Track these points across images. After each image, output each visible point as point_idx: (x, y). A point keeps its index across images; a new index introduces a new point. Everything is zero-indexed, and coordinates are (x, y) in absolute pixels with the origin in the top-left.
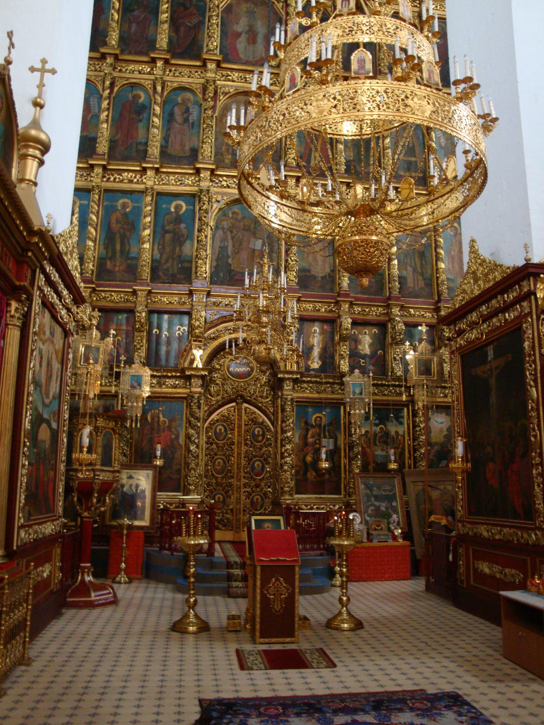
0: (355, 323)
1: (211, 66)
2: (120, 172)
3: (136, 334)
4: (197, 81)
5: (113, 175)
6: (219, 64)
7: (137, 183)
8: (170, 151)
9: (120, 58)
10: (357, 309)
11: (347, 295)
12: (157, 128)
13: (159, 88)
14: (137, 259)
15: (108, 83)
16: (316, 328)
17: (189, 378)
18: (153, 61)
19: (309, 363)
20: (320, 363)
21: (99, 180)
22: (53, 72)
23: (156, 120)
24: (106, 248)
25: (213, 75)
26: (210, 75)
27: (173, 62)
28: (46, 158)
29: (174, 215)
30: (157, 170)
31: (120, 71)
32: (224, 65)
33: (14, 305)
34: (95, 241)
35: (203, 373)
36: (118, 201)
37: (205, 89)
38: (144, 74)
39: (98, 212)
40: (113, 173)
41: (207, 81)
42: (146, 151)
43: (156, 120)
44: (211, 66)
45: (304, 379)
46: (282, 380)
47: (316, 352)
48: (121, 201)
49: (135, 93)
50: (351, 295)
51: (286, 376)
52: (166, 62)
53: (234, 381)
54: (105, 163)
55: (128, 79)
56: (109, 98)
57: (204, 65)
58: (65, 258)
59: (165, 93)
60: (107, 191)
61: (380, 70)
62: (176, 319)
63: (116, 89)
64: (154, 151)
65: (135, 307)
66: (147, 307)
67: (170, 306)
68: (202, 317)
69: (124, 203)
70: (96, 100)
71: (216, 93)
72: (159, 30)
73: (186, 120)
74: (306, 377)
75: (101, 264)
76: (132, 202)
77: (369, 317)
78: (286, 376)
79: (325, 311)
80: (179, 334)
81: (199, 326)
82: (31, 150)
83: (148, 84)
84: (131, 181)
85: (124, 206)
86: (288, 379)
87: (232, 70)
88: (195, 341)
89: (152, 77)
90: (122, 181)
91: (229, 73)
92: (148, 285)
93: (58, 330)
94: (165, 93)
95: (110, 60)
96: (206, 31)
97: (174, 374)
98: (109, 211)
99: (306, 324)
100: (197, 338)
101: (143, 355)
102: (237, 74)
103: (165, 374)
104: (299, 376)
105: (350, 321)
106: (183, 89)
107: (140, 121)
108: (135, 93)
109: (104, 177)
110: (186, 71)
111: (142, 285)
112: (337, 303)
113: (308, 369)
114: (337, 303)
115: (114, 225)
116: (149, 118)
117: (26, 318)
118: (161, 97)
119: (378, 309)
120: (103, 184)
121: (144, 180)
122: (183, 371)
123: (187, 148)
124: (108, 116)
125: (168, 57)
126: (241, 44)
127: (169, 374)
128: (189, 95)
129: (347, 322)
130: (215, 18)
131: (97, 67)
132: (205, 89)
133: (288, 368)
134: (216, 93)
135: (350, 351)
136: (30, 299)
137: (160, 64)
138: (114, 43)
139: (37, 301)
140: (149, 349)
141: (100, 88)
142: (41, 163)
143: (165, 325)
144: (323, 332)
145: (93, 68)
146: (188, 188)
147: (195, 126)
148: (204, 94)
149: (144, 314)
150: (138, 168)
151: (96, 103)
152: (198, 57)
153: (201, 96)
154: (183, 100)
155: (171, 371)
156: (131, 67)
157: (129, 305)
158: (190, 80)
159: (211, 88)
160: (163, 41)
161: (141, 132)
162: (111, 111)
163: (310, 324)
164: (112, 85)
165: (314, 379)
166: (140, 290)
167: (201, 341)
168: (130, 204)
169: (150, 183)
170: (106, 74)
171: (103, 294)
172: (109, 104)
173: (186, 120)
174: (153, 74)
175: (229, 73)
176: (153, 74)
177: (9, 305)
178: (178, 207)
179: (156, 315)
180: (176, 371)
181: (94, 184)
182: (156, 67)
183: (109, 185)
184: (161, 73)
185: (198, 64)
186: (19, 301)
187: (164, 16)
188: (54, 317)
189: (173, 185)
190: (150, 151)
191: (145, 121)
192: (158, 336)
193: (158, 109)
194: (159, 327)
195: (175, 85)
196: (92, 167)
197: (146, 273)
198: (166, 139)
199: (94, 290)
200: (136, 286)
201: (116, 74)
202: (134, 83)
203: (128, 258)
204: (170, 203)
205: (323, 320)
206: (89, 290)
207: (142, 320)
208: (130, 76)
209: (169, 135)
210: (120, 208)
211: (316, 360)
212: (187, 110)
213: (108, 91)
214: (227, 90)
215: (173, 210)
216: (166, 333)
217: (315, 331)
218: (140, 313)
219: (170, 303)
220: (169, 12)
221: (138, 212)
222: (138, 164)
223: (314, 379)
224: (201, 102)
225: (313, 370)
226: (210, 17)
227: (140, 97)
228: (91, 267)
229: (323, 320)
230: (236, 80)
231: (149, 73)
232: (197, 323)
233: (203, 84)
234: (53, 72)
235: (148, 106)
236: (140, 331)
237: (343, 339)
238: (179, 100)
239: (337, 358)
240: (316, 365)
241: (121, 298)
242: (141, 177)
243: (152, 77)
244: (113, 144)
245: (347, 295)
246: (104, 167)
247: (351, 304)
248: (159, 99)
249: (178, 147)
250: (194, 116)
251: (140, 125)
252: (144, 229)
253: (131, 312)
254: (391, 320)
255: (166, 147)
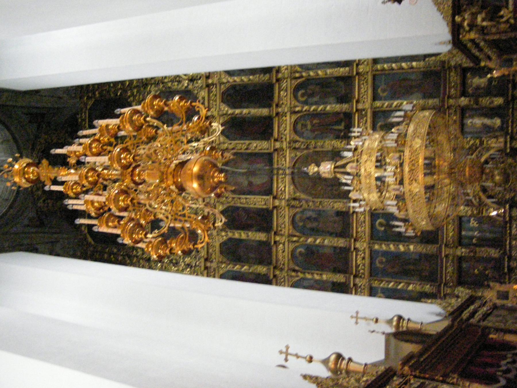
0: (464, 93)
1: (277, 202)
2: (357, 266)
3: (477, 255)
4: (287, 213)
5: (359, 271)
6: (275, 198)
7: (365, 253)
8: (339, 229)
9: (275, 265)
10: (453, 91)
11: (443, 101)
12: (324, 240)
13: (295, 239)
14: (420, 254)
15: (293, 274)
16: (469, 122)
17: (511, 217)
18: (275, 242)
19: (496, 126)
20: (496, 118)
21: (364, 280)
22: (357, 313)
23: (318, 241)
24: (413, 275)
25: (283, 202)
26: (283, 203)
27: (275, 229)
28: (406, 318)
29: (387, 228)
30: (355, 240)
31: (284, 264)
32: (275, 194)
33: (491, 336)
34: (409, 284)
35: (507, 206)
36: (378, 268)
37: (293, 207)
38: (284, 248)
39: (387, 282)
40: (358, 270)
41: (288, 205)
42: (341, 248)
43: (318, 241)
44: (277, 202)
45: (510, 131)
46: (512, 148)
47: (487, 121)
48: (378, 265)
49: (298, 255)
50: (442, 95)
51: (508, 145)
52: (275, 234)
53: (512, 183)
54: (352, 277)
55: (288, 260)
56: (304, 273)
57: (275, 207)
58: (455, 308)
59: (298, 234)
60: (371, 275)
61: (268, 80)
62: (465, 225)
63: (297, 268)
64: (341, 243)
65: (457, 256)
66: (457, 247)
67: (456, 230)
68: (464, 209)
69: (380, 262)
70: (305, 282)
71: (295, 199)
72: (253, 238)
73: (316, 219)
74: (508, 130)
75: (424, 279)
76: (377, 257)
77: (458, 81)
78: (508, 145)
79: (456, 116)
80: (477, 224)
81: (472, 210)
82: (404, 324)
83: (292, 246)
84: (364, 258)
85: (381, 262)
86: (510, 144)
87: (278, 188)
88: (482, 213)
89: (286, 244)
90: (364, 265)
91: (280, 189)
92: (441, 247)
93: (495, 312)
94: (298, 234)
95: (277, 272)
96: (252, 206)
97: (508, 228)
98: (385, 274)
99: (466, 130)
100: (480, 212)
101: (493, 251)
102: (280, 185)
103: (508, 235)
104: (508, 137)
105: (463, 99)
106: (293, 222)
107: (318, 251)
108: (298, 255)
109: (361, 277)
110: (281, 221)
111: (441, 252)
112: (449, 108)
113: (501, 128)
114: (449, 108)
115: (396, 270)
116: (317, 246)
117: (497, 330)
118: (300, 237)
119: (452, 76)
120: (366, 277)
121: (363, 248)
122: (506, 223)
123: (337, 219)
124: (317, 274)
125: (273, 233)
126: (258, 181)
127: (508, 231)
128: (298, 217)
129: (464, 101)
130: (242, 201)
131: (282, 280)
132: (293, 207)
133: (502, 145)
134: (295, 199)
135: (486, 96)
136: (487, 328)
137: (278, 238)
138: (265, 269)
139: (485, 323)
140: (489, 246)
141: (297, 278)
142: (409, 320)
143: (470, 233)
144: (472, 117)
145: (283, 284)
146: (367, 218)
147: (319, 213)
148: (297, 207)
149: (463, 250)
150: (354, 254)
151: (307, 282)
152: (272, 212)
153: (298, 210)
154: (301, 222)
155: (506, 231)
156: (280, 258)
157: (455, 259)
158: (287, 217)
159: (293, 203)
160: (261, 236)
161: (326, 251)
162: (313, 271)
163: (465, 127)
164: (294, 271)
165: (510, 124)
166: (445, 252)
167: (483, 209)
168: (379, 258)
169: (365, 245)
170: (287, 275)
171: (448, 278)
172: (309, 273)
173: (316, 219)
174: (284, 242)
175: (280, 189)
176: (284, 242)
177: (492, 339)
178: (381, 224)
179: (463, 241)
180: (506, 228)
181: (367, 284)
182: (279, 241)
183: (367, 274)
184: (284, 238)
185: (275, 212)
186: (489, 333)
187: (244, 236)
188: (489, 315)
189: (365, 228)
190: (342, 245)
191: (319, 248)
192: (479, 239)
193: (310, 240)
194: (472, 238)
195: (291, 227)
196: (355, 285)
197: (431, 249)
198: (331, 234)
199: (445, 284)
200: (441, 256)
201: (286, 269)
202: (292, 255)
203: (420, 259)
204: (378, 231)
205: (463, 117)
206: (445, 288)
207: (468, 251)
208: (286, 259)
209: (328, 232)
210: (383, 266)
211: (494, 121)
212: (309, 218)
213: (299, 274)
214: (292, 191)
215: (383, 229)
216: (476, 233)
217: (471, 123)
218: (462, 253)
219: (453, 230)
220: (239, 231)
221: (385, 253)
222: (350, 254)
223: (510, 124)
224: (301, 210)
225: (503, 123)
226: (241, 203)
227: (300, 251)
228: (428, 286)
229: (463, 117)
230: (284, 185)
231: (284, 244)
232: (470, 213)
233: (289, 209)
234: (357, 313)
235: (306, 246)
236: (476, 252)
237: (477, 103)
238: (301, 224)
239: (492, 106)
240: (498, 122)
241: (450, 265)
242: (361, 251)
243: (286, 244)
244: (336, 271)
245: (443, 101)
246: (355, 276)
247: (449, 97)
248: (302, 239)
249: (336, 226)
250: (314, 215)
251: (321, 251)
252: (399, 248)
253: (460, 259)
254: (460, 65)
255: (337, 234)
